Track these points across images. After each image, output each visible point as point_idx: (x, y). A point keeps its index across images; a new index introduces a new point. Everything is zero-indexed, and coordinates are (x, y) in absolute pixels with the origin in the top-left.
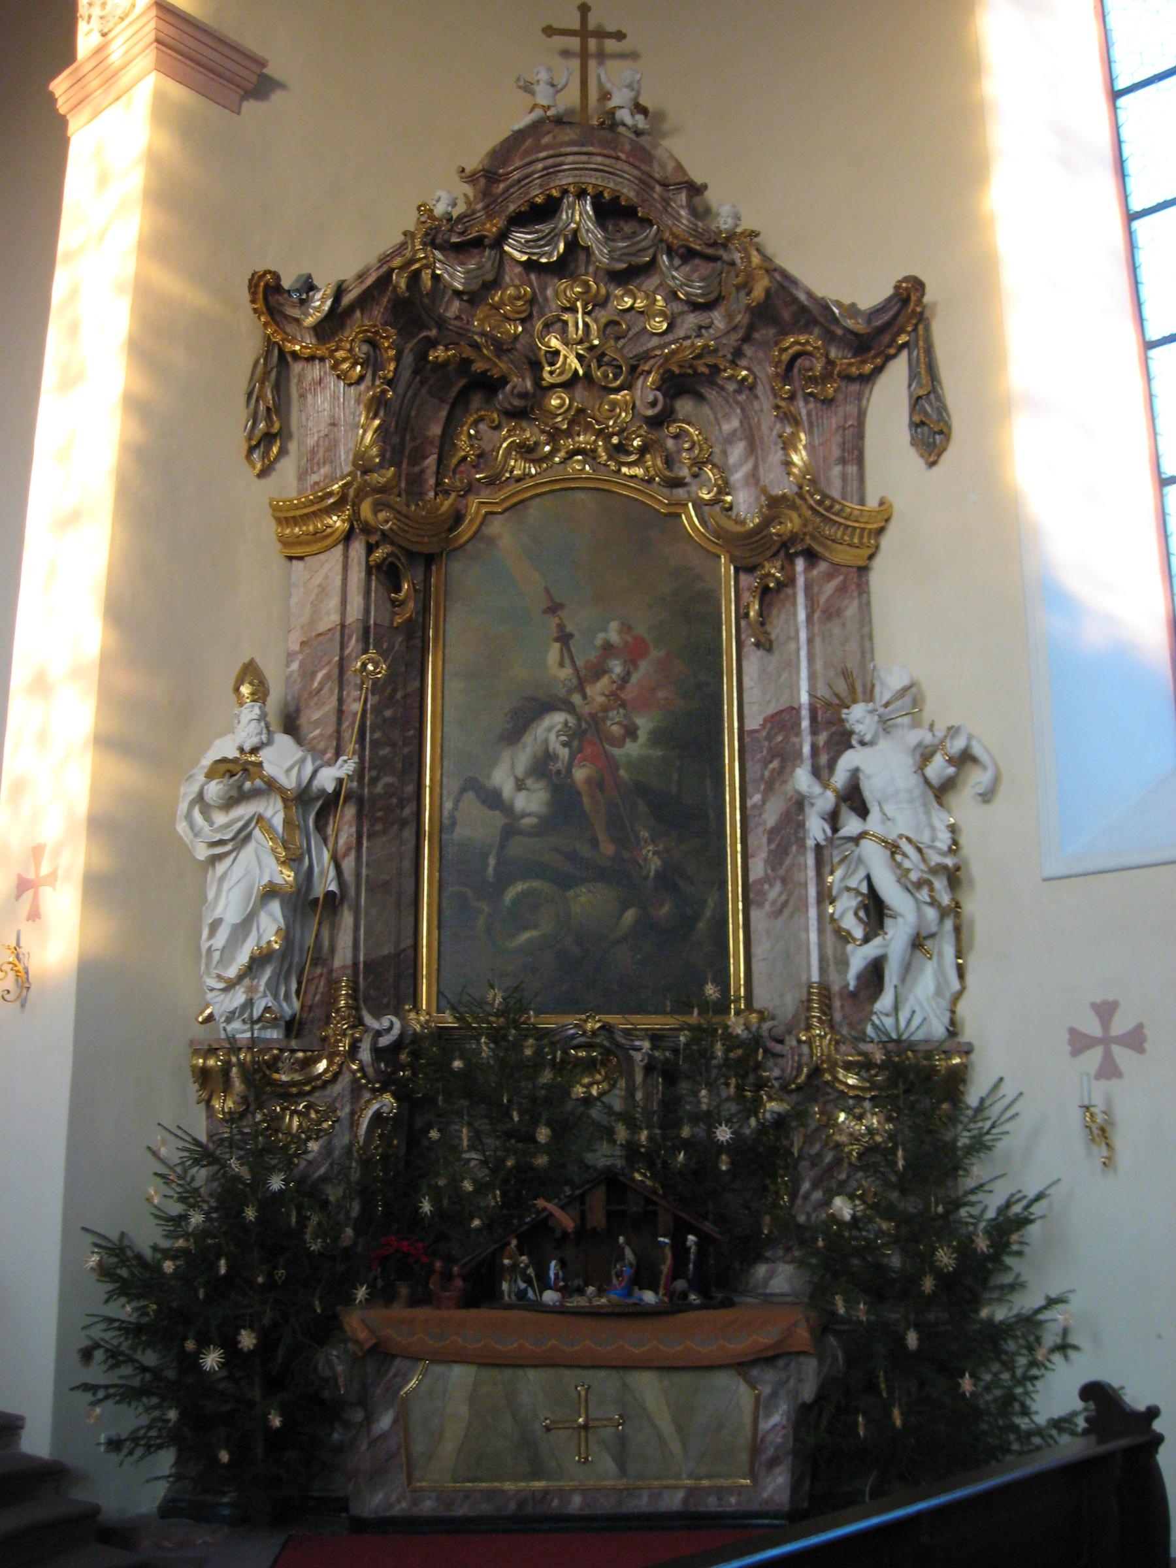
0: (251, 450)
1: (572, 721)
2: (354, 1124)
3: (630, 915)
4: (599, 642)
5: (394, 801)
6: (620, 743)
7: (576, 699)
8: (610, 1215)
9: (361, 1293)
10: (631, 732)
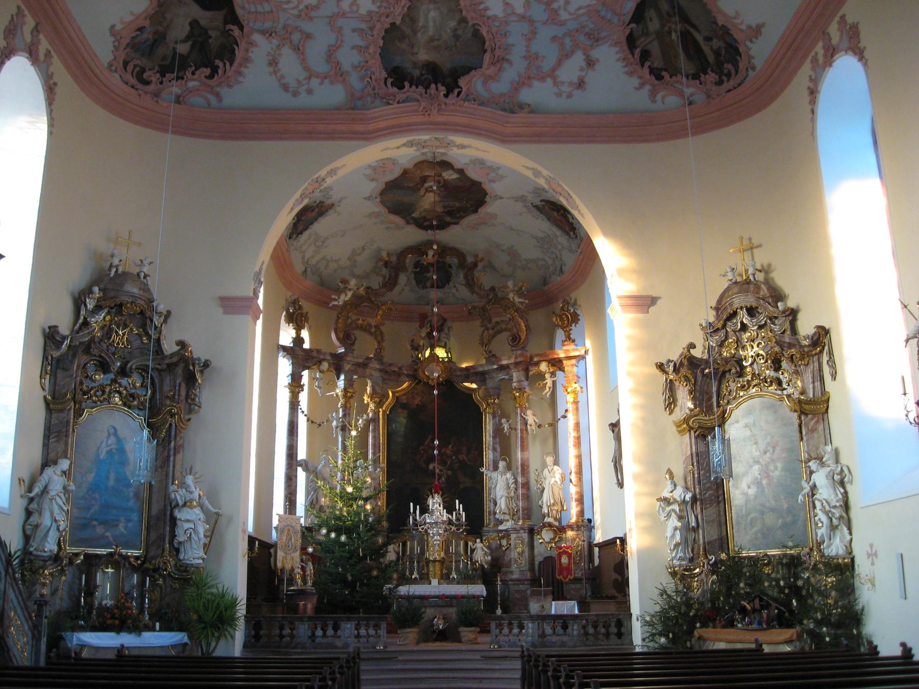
0: (666, 409)
1: (760, 467)
2: (707, 583)
3: (780, 521)
4: (765, 443)
5: (713, 498)
6: (773, 471)
7: (761, 460)
8: (760, 605)
9: (698, 625)
10: (776, 468)
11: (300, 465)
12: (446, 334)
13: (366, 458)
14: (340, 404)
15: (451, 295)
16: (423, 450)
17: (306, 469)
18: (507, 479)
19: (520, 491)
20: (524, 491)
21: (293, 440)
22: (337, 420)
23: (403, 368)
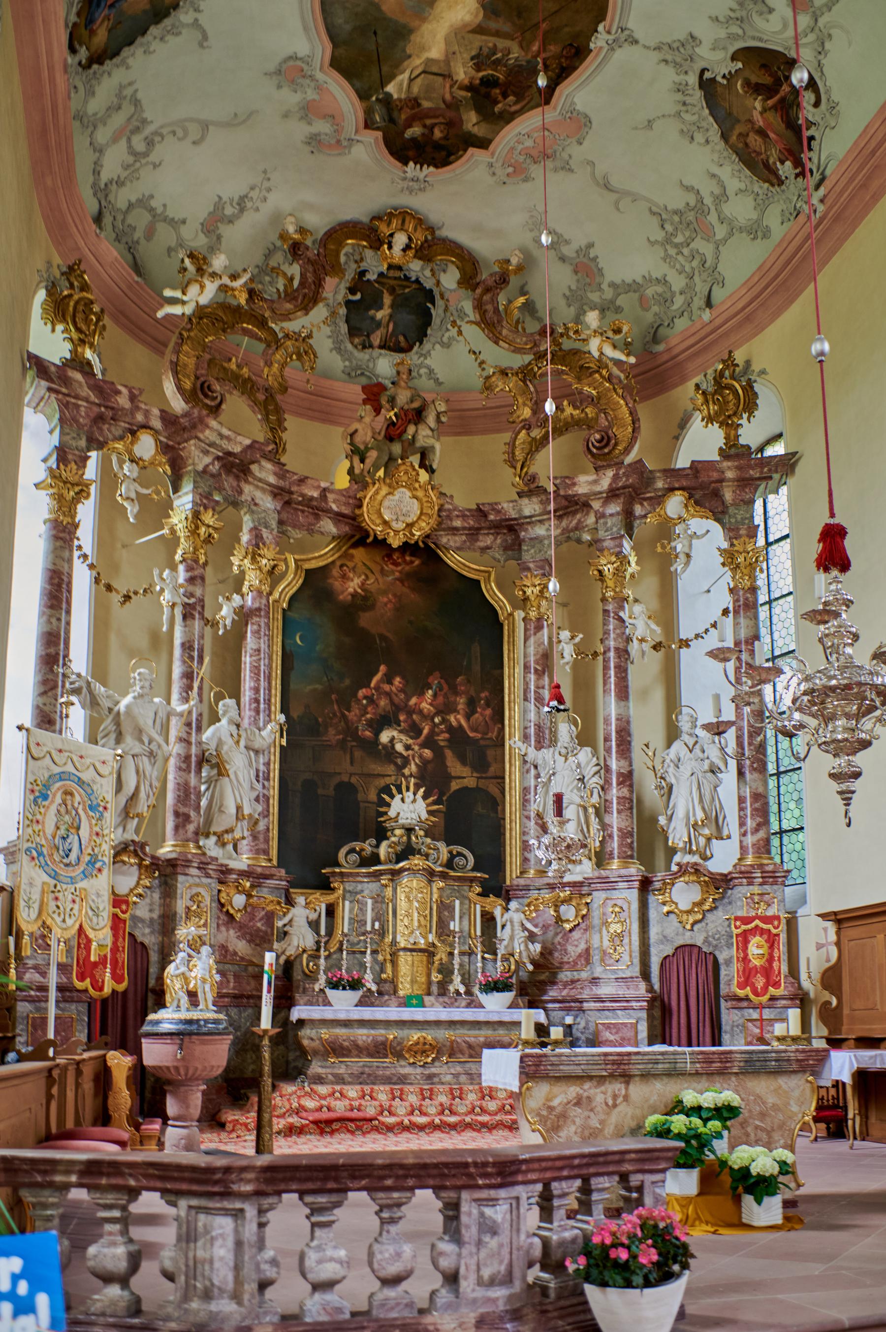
11: (76, 691)
12: (432, 430)
13: (236, 695)
14: (180, 552)
15: (423, 371)
16: (365, 697)
17: (93, 703)
18: (579, 766)
19: (614, 792)
20: (625, 792)
21: (59, 620)
22: (176, 588)
23: (330, 497)
